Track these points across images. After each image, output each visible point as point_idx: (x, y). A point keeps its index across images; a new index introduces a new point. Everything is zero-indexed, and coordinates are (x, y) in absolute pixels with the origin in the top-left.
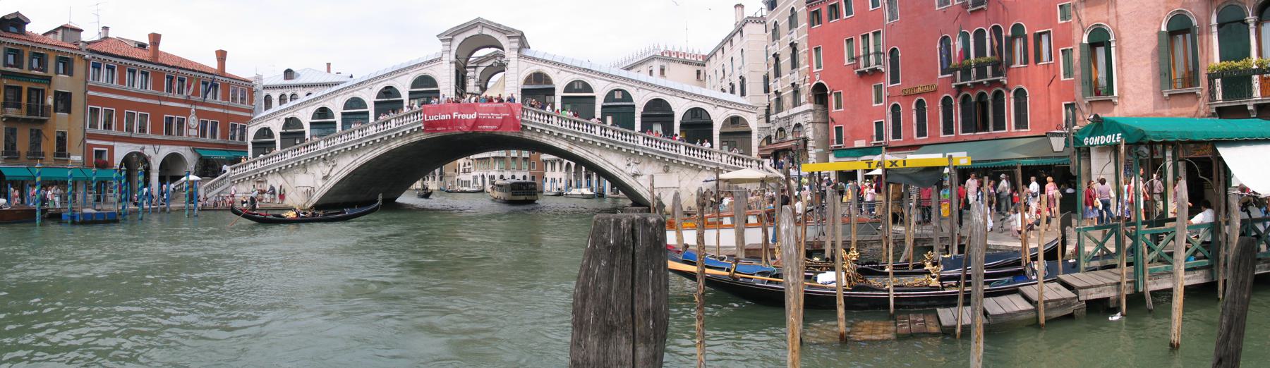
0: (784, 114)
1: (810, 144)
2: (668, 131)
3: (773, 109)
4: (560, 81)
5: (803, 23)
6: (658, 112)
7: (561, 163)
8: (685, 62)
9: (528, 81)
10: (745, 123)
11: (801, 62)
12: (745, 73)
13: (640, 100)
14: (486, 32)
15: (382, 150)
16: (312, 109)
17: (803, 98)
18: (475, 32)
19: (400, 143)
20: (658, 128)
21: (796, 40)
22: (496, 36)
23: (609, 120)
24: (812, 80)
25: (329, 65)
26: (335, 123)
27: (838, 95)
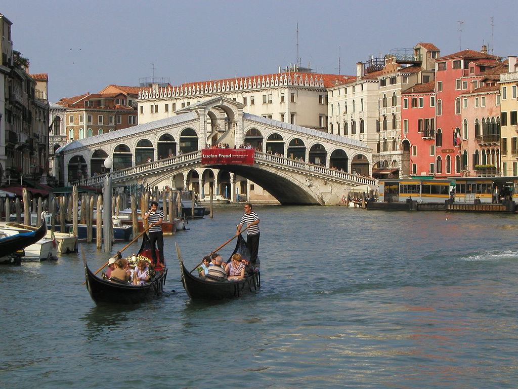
0: (388, 153)
1: (400, 172)
2: (323, 162)
3: (382, 148)
4: (266, 133)
5: (399, 106)
6: (318, 152)
8: (310, 89)
9: (248, 133)
11: (398, 126)
14: (225, 104)
16: (114, 145)
17: (398, 147)
20: (318, 160)
22: (230, 106)
23: (292, 155)
24: (402, 139)
27: (415, 148)
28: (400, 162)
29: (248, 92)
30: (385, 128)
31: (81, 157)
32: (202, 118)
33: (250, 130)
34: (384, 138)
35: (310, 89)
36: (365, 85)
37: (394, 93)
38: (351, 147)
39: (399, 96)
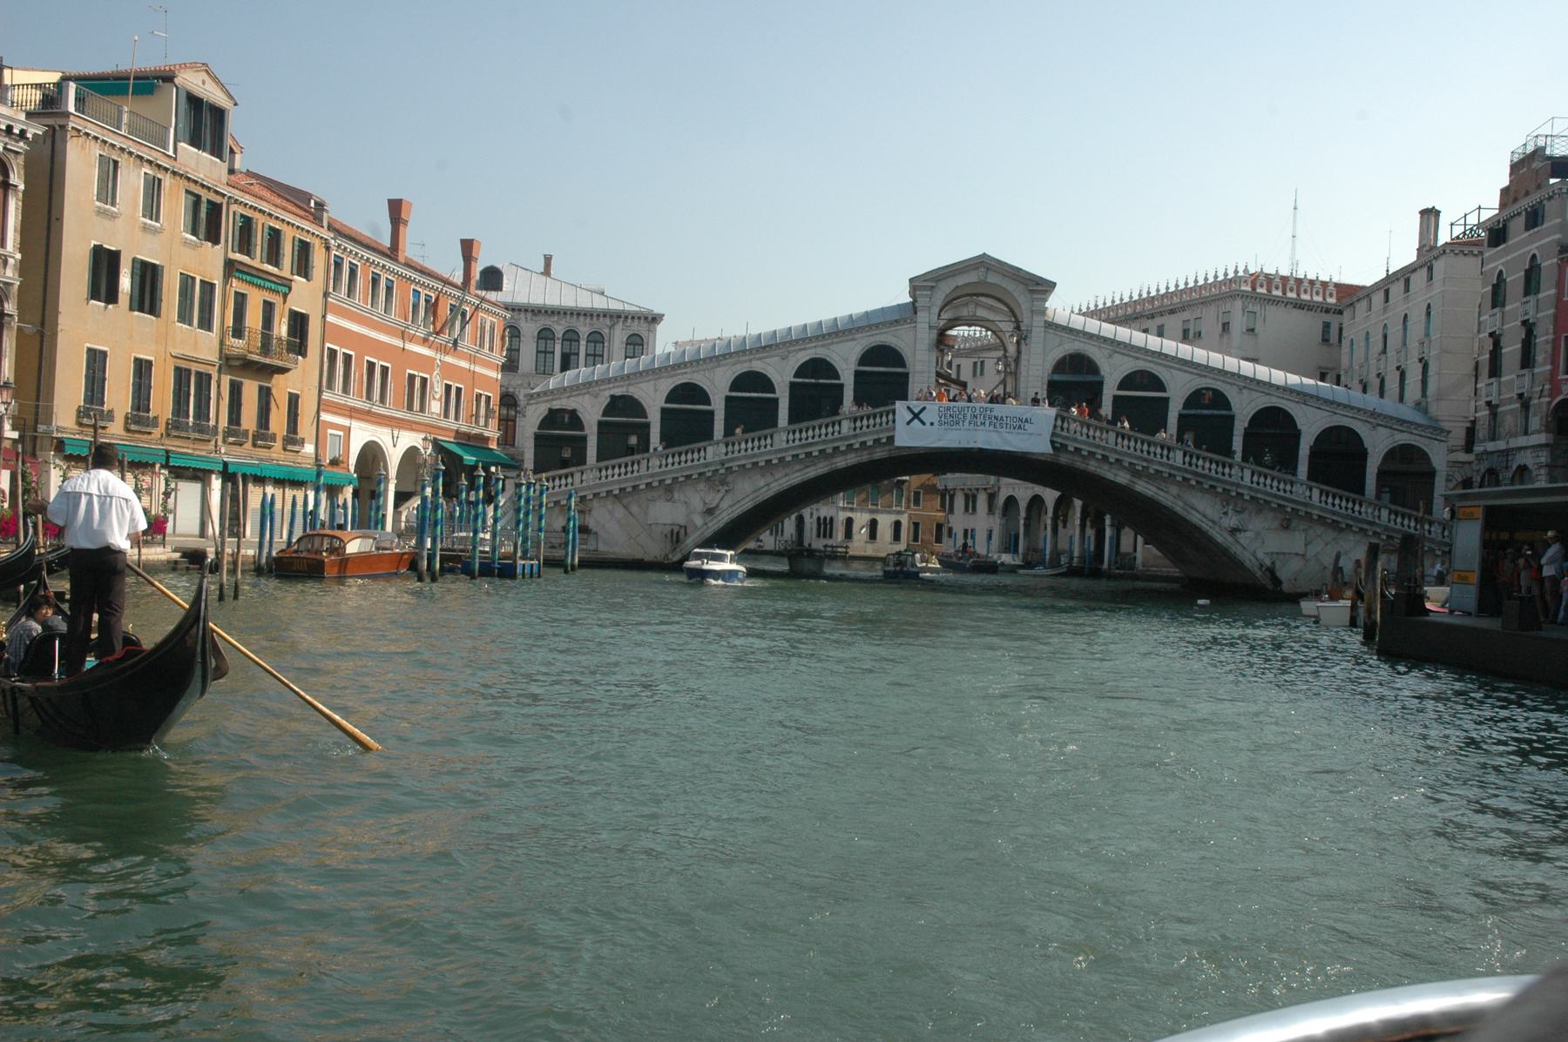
0: (1501, 445)
3: (1482, 432)
5: (1548, 292)
7: (992, 497)
9: (1060, 366)
10: (1424, 456)
11: (1540, 358)
12: (1432, 354)
13: (1244, 408)
14: (992, 278)
15: (820, 469)
16: (667, 385)
17: (1535, 422)
18: (972, 277)
19: (852, 459)
21: (1531, 318)
22: (1010, 286)
23: (1189, 436)
24: (1552, 395)
25: (548, 260)
26: (712, 413)
28: (1543, 471)
29: (1152, 317)
30: (1495, 370)
31: (573, 413)
32: (922, 316)
33: (1064, 358)
34: (1489, 403)
35: (1299, 305)
36: (1439, 266)
37: (1534, 256)
38: (1377, 419)
39: (1548, 263)
